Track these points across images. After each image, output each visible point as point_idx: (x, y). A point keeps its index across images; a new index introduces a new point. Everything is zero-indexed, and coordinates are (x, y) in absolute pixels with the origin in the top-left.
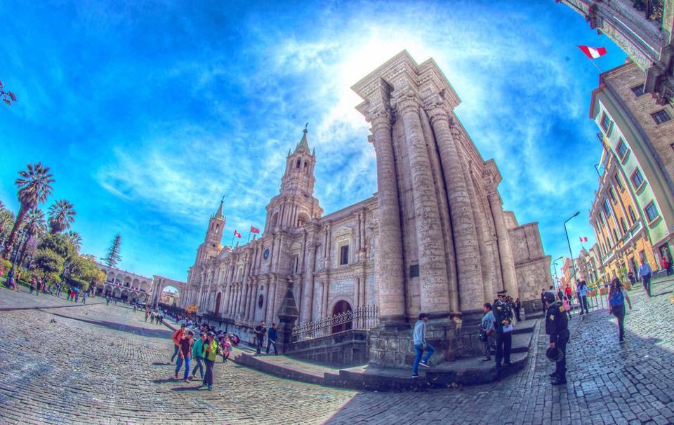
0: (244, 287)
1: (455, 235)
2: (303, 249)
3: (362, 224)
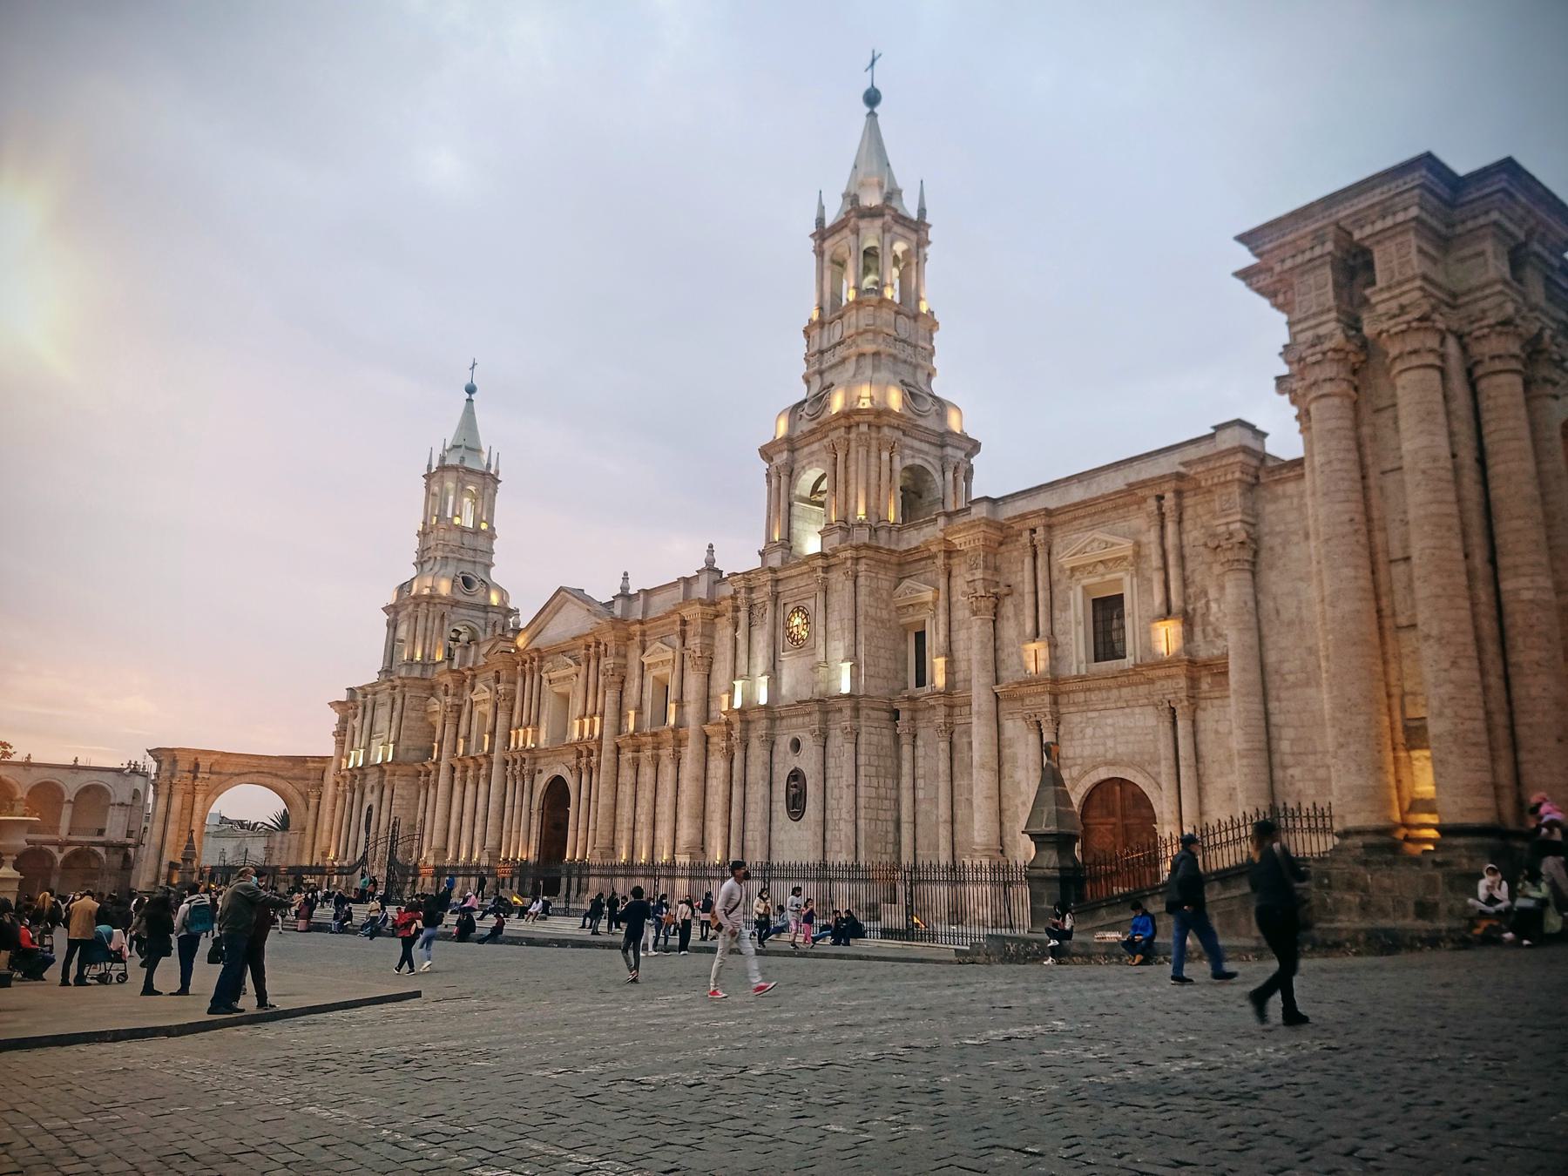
0: (690, 752)
1: (1511, 670)
2: (942, 603)
3: (1171, 528)
